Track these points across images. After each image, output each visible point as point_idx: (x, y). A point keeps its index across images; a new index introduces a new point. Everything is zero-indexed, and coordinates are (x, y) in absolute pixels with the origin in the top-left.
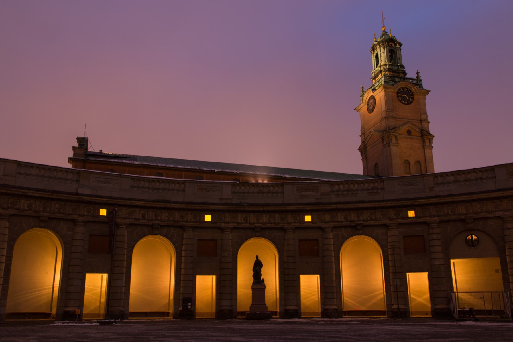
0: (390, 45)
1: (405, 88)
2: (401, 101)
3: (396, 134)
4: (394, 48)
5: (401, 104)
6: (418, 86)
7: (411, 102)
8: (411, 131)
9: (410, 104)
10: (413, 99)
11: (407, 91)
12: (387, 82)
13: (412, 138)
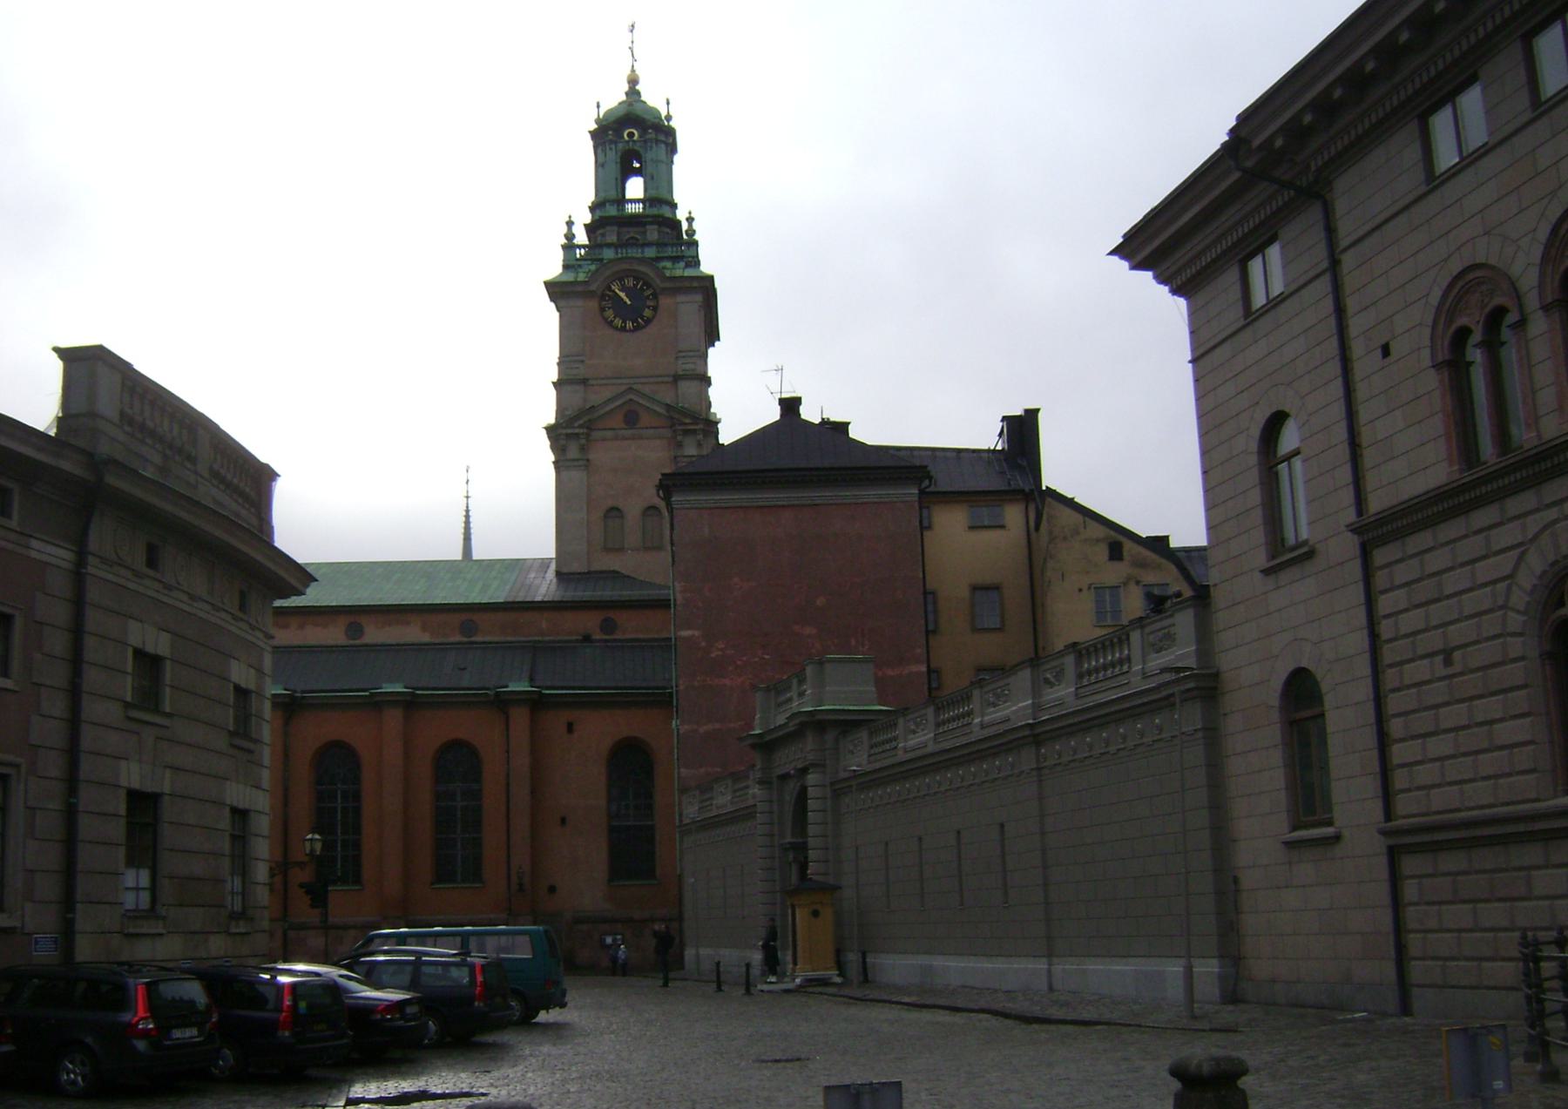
2: (610, 324)
3: (577, 431)
6: (682, 264)
7: (648, 321)
9: (644, 327)
10: (655, 309)
13: (641, 438)
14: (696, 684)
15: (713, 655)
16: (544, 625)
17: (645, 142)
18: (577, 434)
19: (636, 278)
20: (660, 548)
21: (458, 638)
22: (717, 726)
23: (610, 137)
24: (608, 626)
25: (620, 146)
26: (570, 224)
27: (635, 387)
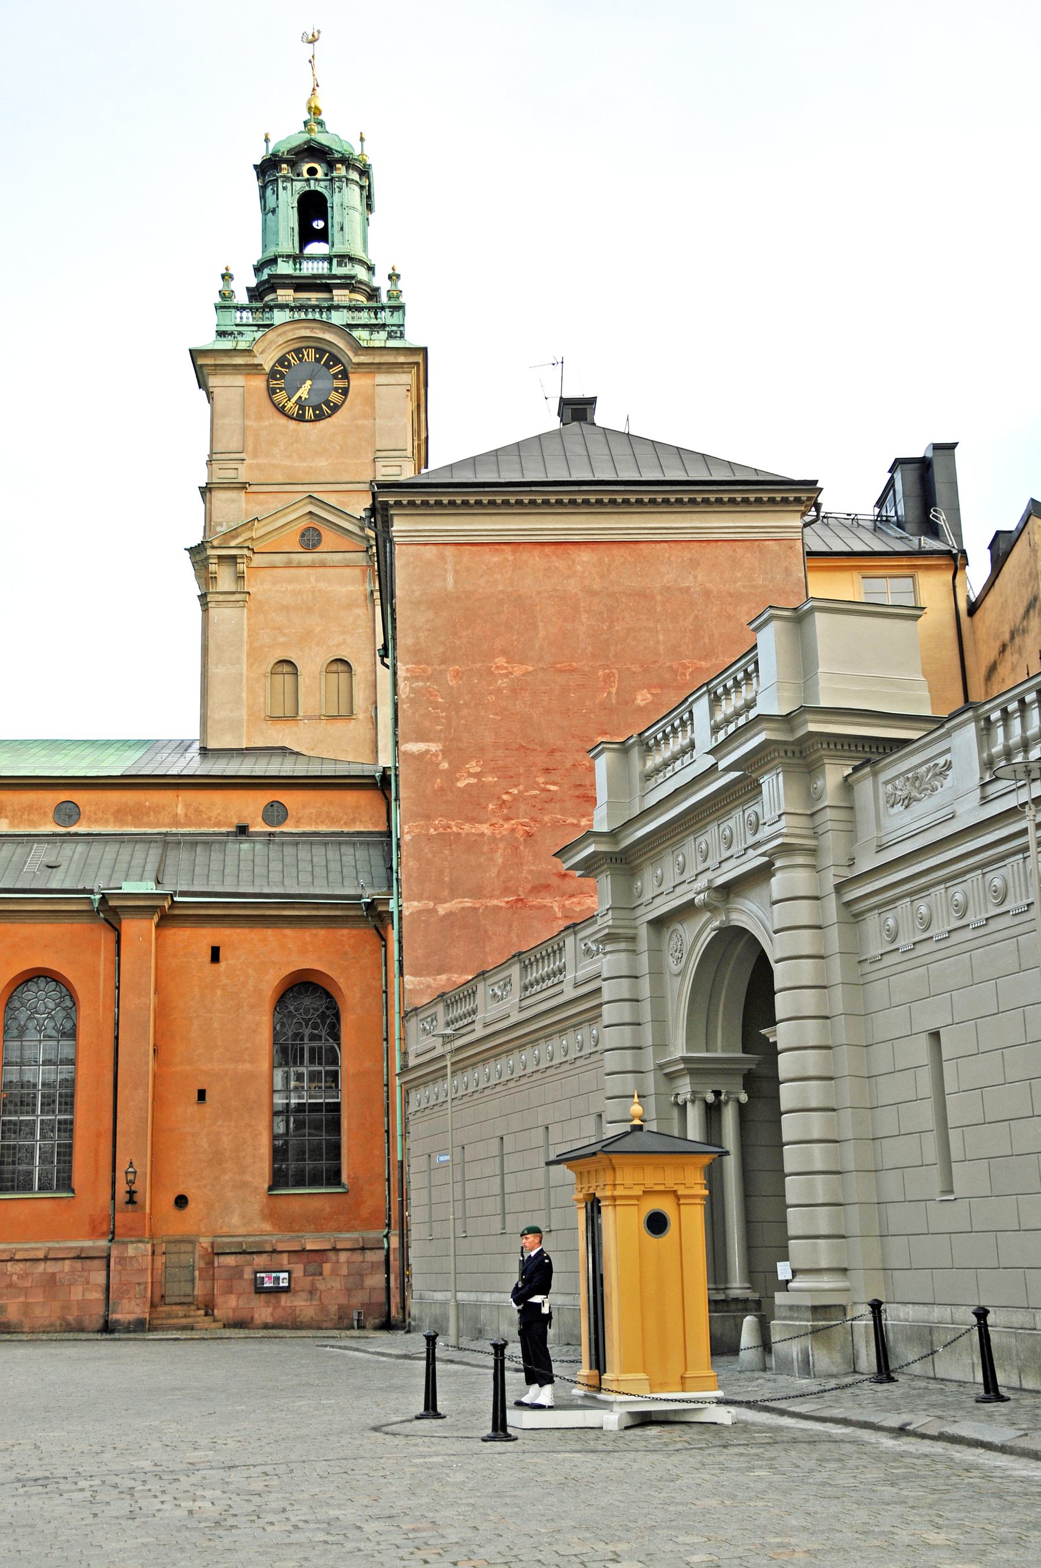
0: (306, 176)
1: (306, 348)
4: (322, 184)
5: (283, 420)
7: (335, 408)
8: (319, 535)
9: (330, 416)
10: (345, 392)
11: (318, 360)
12: (231, 333)
13: (323, 565)
14: (432, 831)
15: (461, 784)
16: (180, 810)
17: (331, 180)
18: (234, 557)
19: (318, 350)
20: (350, 715)
21: (51, 828)
22: (468, 903)
23: (284, 172)
24: (275, 813)
25: (299, 187)
26: (226, 277)
27: (314, 495)
